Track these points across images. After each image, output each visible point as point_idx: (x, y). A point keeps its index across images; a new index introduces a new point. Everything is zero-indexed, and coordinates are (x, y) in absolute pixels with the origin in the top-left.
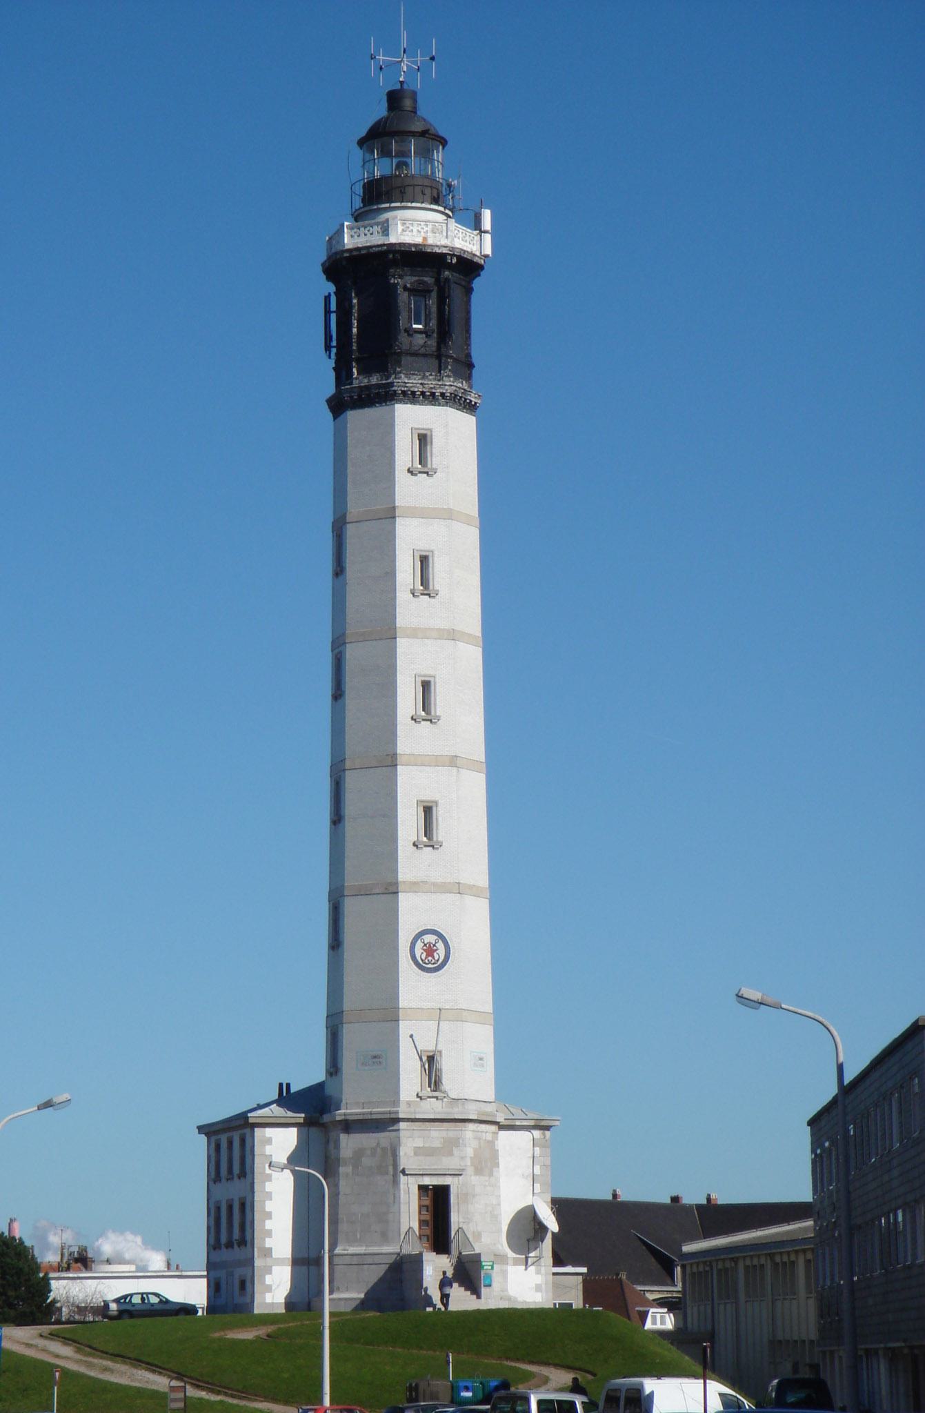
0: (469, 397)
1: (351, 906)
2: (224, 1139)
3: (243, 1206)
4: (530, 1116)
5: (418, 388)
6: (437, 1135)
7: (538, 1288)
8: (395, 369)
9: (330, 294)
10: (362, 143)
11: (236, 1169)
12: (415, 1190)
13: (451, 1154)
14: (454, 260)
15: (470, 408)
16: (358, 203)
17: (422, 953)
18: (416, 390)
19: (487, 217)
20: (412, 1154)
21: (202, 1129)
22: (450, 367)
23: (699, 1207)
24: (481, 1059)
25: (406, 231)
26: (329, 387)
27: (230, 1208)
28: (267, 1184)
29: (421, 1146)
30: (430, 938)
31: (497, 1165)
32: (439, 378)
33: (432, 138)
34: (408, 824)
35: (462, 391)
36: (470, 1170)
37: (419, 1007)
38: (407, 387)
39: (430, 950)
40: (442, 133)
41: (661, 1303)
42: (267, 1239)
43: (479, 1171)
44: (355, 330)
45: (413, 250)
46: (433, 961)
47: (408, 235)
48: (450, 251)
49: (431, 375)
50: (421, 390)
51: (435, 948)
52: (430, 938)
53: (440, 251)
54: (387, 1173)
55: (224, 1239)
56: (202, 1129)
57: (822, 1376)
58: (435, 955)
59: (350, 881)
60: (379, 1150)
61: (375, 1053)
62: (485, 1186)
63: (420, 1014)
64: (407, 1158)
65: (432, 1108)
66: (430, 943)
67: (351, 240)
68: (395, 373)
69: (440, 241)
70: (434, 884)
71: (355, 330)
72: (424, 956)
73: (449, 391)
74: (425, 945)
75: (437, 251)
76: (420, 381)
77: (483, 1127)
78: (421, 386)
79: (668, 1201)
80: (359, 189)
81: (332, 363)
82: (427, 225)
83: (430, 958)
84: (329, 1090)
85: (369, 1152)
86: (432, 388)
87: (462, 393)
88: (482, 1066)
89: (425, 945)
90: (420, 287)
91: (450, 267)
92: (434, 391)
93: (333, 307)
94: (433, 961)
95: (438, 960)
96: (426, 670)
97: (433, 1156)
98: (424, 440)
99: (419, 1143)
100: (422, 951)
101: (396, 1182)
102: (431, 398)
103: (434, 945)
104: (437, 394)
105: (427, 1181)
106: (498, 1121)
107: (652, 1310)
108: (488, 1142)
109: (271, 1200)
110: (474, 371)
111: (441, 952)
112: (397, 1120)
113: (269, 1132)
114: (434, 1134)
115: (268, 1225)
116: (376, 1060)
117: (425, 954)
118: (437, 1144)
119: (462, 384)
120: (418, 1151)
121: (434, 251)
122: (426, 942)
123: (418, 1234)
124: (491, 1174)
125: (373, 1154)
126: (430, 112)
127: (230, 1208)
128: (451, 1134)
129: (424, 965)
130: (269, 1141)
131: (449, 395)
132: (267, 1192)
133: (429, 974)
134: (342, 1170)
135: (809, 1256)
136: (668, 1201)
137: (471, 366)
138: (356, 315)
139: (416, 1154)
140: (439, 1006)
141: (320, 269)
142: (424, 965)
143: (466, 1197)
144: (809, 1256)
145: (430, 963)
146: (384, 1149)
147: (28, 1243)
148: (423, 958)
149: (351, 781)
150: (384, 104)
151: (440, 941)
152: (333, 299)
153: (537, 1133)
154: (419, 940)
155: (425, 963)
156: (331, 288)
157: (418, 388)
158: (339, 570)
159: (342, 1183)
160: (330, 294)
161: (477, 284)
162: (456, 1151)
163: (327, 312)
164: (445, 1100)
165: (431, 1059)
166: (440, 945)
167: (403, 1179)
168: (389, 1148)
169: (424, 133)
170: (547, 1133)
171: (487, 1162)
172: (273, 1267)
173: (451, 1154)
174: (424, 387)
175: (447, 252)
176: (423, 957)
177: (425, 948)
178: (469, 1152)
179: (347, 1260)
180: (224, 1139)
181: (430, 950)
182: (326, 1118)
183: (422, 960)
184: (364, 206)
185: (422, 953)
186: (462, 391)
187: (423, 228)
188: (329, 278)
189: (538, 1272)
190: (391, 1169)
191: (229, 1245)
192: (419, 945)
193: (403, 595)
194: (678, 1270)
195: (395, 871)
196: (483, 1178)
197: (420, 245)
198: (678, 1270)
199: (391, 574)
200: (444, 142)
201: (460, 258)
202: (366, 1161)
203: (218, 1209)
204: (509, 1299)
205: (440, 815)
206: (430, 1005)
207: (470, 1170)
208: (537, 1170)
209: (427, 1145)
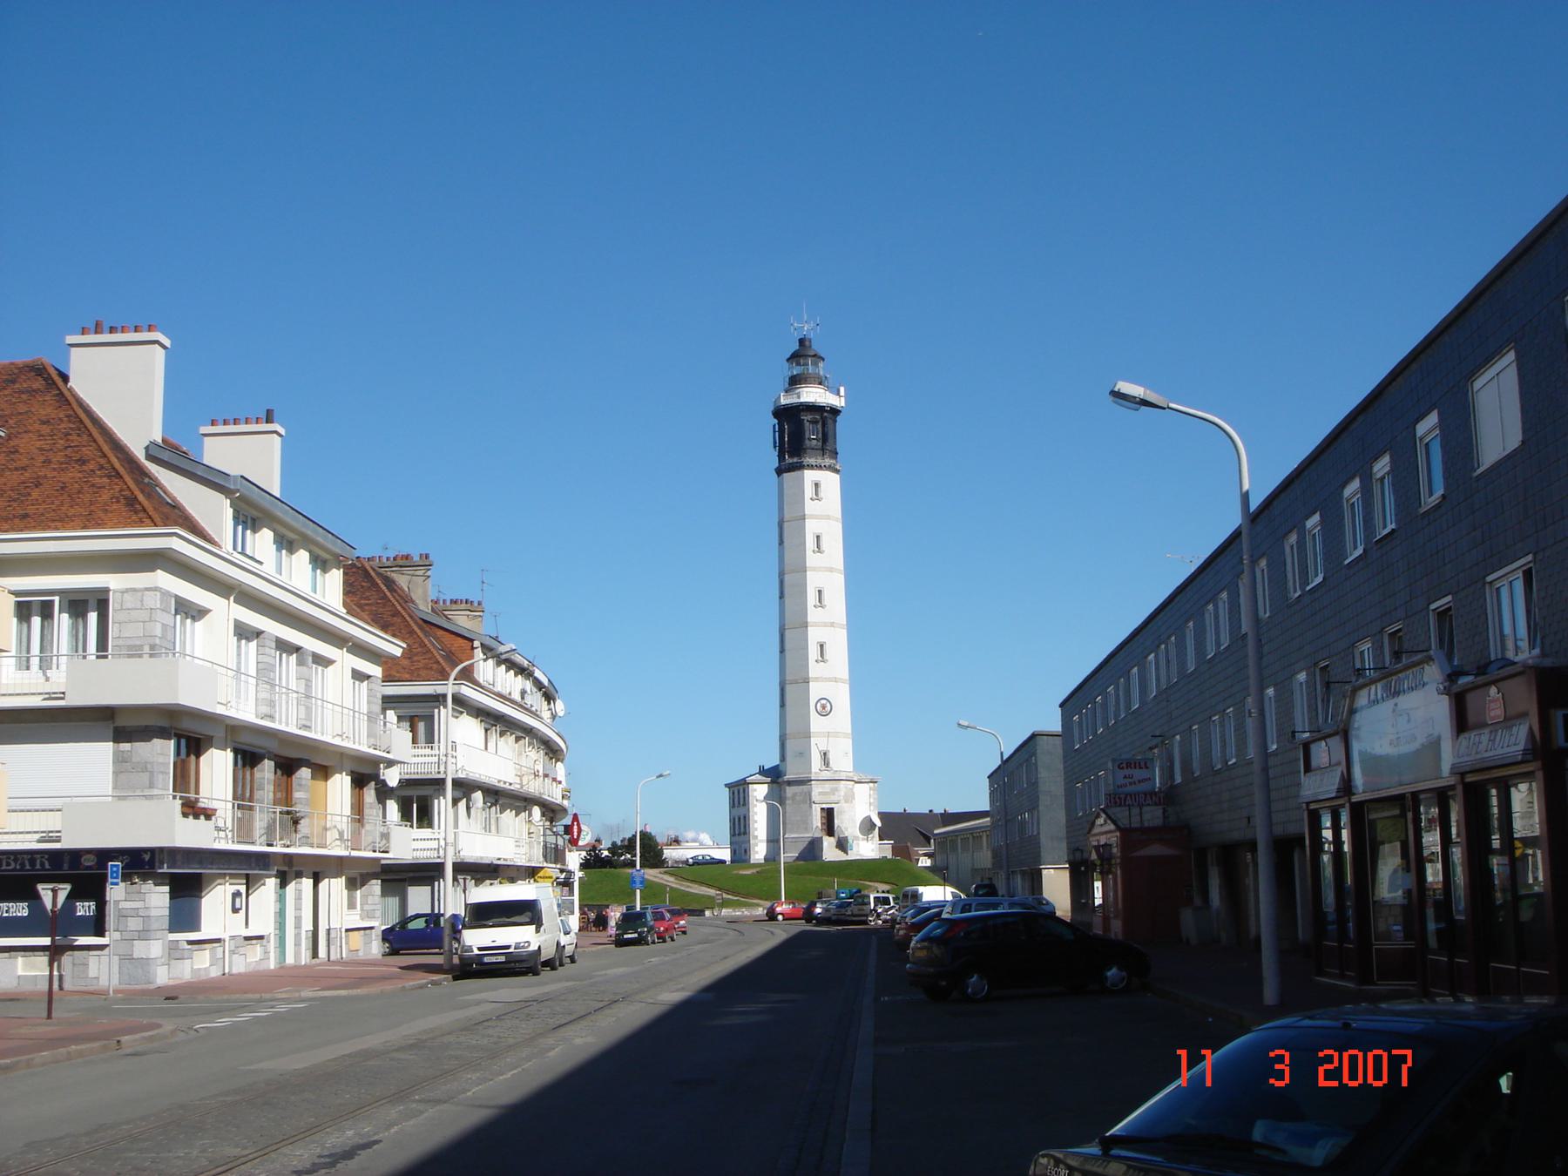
1: (788, 688)
2: (736, 789)
3: (745, 817)
4: (869, 777)
6: (828, 786)
10: (788, 360)
11: (741, 803)
12: (819, 810)
13: (834, 794)
15: (837, 471)
16: (787, 385)
19: (842, 390)
21: (726, 785)
23: (941, 814)
26: (774, 462)
27: (739, 819)
30: (824, 702)
31: (854, 799)
33: (818, 357)
34: (813, 652)
36: (843, 801)
39: (824, 707)
41: (925, 855)
43: (846, 802)
44: (786, 439)
52: (824, 702)
55: (737, 832)
56: (726, 785)
57: (994, 882)
59: (789, 677)
63: (820, 734)
64: (815, 796)
65: (826, 775)
67: (784, 401)
71: (786, 439)
79: (928, 812)
80: (787, 379)
84: (781, 768)
91: (827, 411)
93: (777, 429)
96: (820, 585)
98: (817, 485)
101: (811, 807)
102: (820, 467)
105: (824, 806)
107: (921, 858)
110: (838, 456)
112: (812, 780)
113: (755, 786)
114: (827, 786)
115: (756, 825)
120: (820, 793)
124: (852, 802)
126: (816, 347)
127: (739, 819)
128: (835, 786)
130: (755, 790)
134: (787, 802)
135: (988, 833)
136: (928, 812)
137: (837, 453)
141: (771, 414)
143: (841, 813)
144: (988, 833)
147: (653, 834)
149: (788, 634)
150: (798, 344)
152: (777, 426)
153: (871, 785)
156: (776, 421)
158: (781, 542)
159: (787, 807)
161: (839, 418)
162: (836, 793)
163: (774, 432)
165: (825, 754)
166: (828, 705)
167: (814, 805)
169: (815, 356)
170: (876, 785)
171: (850, 798)
173: (834, 794)
178: (842, 793)
179: (790, 840)
180: (736, 789)
181: (824, 707)
182: (780, 780)
188: (775, 417)
191: (739, 834)
192: (819, 705)
193: (809, 553)
194: (932, 841)
195: (808, 672)
198: (932, 841)
199: (804, 543)
200: (823, 360)
202: (798, 798)
203: (734, 819)
204: (860, 855)
205: (826, 648)
207: (843, 801)
208: (872, 801)
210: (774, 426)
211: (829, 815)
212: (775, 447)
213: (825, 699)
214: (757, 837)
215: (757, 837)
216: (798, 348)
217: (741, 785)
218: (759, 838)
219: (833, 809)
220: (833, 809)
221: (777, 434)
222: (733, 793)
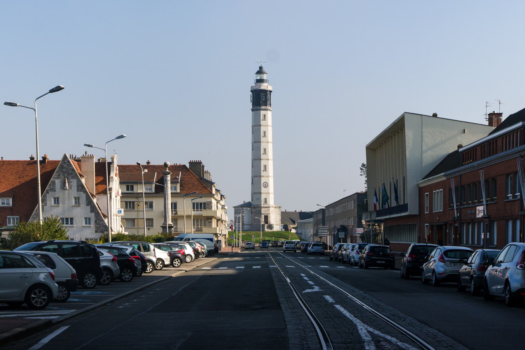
6: (266, 209)
7: (279, 228)
39: (265, 185)
40: (267, 73)
63: (264, 193)
64: (262, 212)
65: (266, 206)
81: (252, 104)
93: (252, 96)
96: (265, 147)
98: (265, 116)
99: (264, 210)
101: (261, 215)
105: (265, 215)
111: (267, 185)
120: (264, 211)
126: (265, 69)
150: (259, 68)
152: (252, 95)
156: (251, 93)
161: (271, 93)
163: (251, 97)
165: (266, 199)
166: (267, 184)
181: (265, 185)
192: (264, 184)
195: (261, 174)
202: (257, 212)
210: (251, 95)
211: (266, 217)
212: (251, 102)
213: (266, 182)
216: (259, 70)
217: (237, 207)
218: (245, 224)
219: (268, 216)
220: (268, 216)
221: (252, 97)
222: (236, 209)
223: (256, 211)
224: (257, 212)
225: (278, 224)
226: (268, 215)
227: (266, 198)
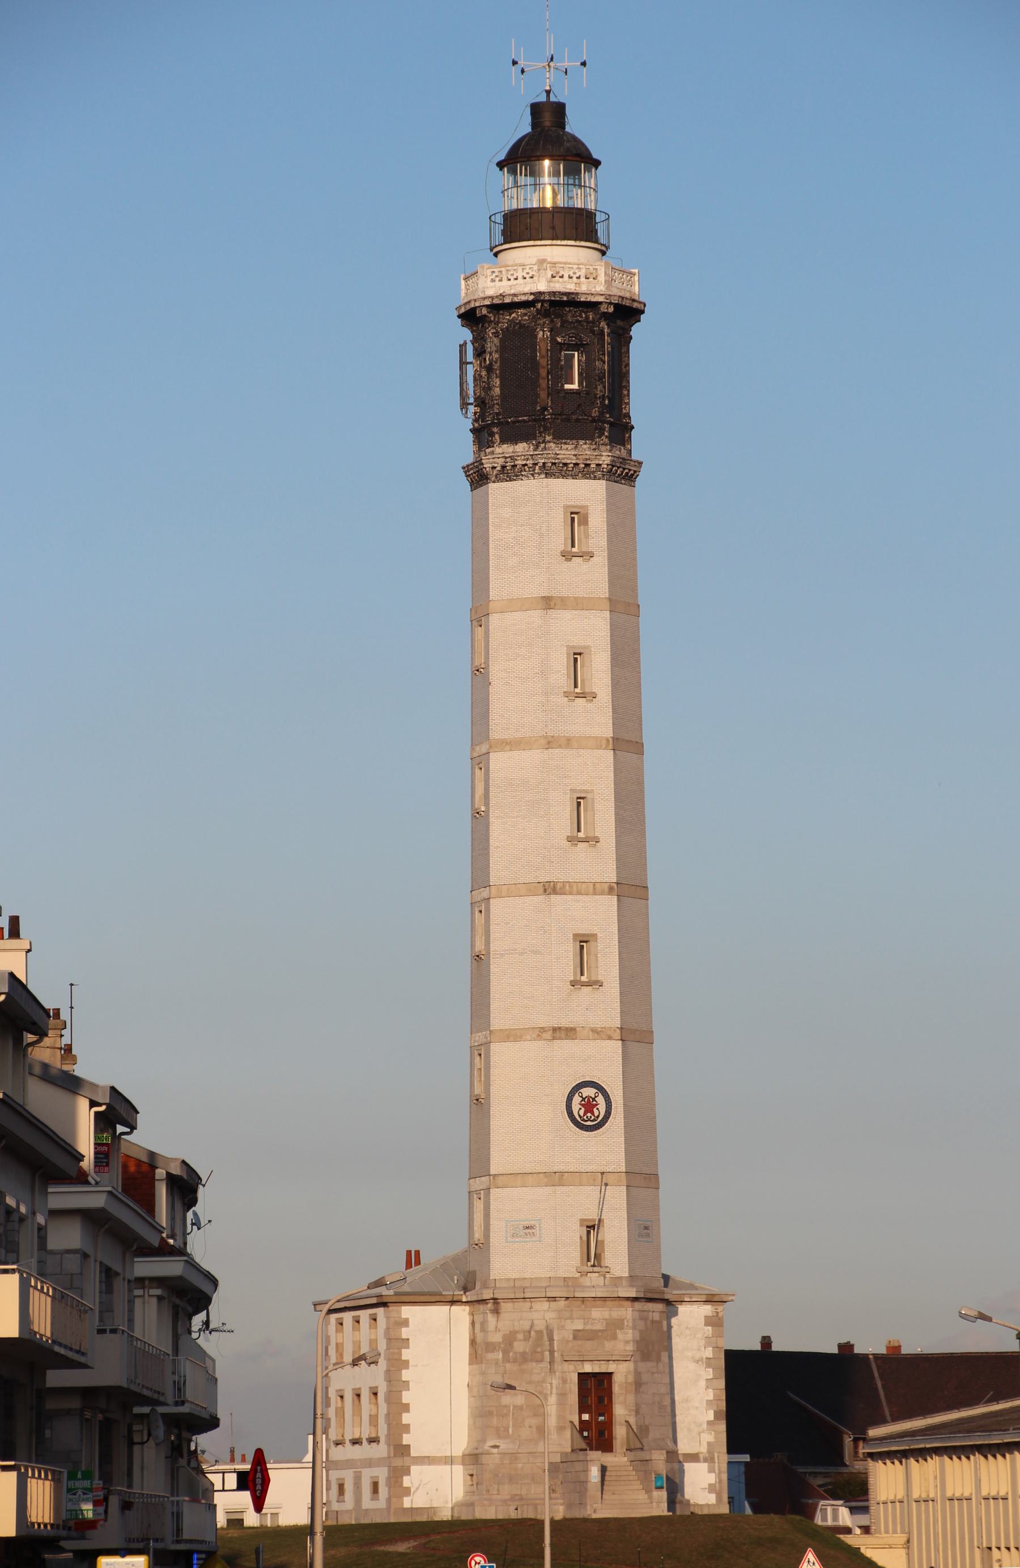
0: (627, 467)
5: (571, 459)
7: (711, 1488)
8: (545, 437)
9: (465, 343)
13: (614, 1337)
14: (611, 309)
17: (580, 1109)
18: (569, 461)
20: (571, 1336)
22: (606, 434)
24: (646, 1228)
25: (555, 277)
28: (404, 1372)
29: (582, 1329)
30: (589, 1092)
32: (594, 447)
35: (621, 460)
37: (577, 1170)
38: (558, 459)
39: (589, 1105)
42: (404, 1435)
45: (565, 298)
46: (593, 1117)
47: (558, 282)
48: (607, 299)
49: (586, 444)
50: (574, 462)
51: (594, 1102)
52: (589, 1092)
53: (595, 300)
54: (542, 1361)
58: (595, 1110)
60: (533, 1333)
61: (527, 1223)
62: (653, 1373)
66: (588, 1097)
68: (544, 442)
69: (595, 287)
70: (594, 1031)
72: (582, 1113)
73: (606, 462)
74: (584, 1099)
75: (592, 300)
76: (573, 453)
77: (650, 1306)
78: (574, 458)
82: (580, 268)
83: (589, 1115)
85: (520, 1336)
86: (587, 460)
87: (621, 463)
88: (648, 1235)
89: (584, 1099)
90: (572, 341)
92: (588, 462)
94: (593, 1117)
95: (599, 1116)
97: (594, 1340)
100: (580, 1107)
103: (594, 1099)
104: (592, 466)
106: (666, 1298)
108: (656, 1322)
109: (409, 1390)
116: (530, 1231)
117: (583, 1109)
118: (598, 1327)
119: (620, 451)
120: (577, 1335)
121: (588, 300)
122: (584, 1097)
123: (578, 1429)
125: (527, 1338)
129: (582, 1122)
131: (605, 466)
132: (404, 1381)
133: (588, 1133)
138: (498, 372)
139: (575, 1338)
140: (601, 1169)
142: (582, 1122)
145: (589, 1120)
146: (539, 1333)
148: (582, 1115)
151: (600, 1094)
154: (577, 1095)
155: (584, 1120)
156: (467, 335)
157: (571, 459)
160: (465, 343)
161: (636, 330)
164: (608, 1275)
166: (601, 1100)
168: (545, 1332)
172: (412, 1467)
173: (614, 1337)
174: (578, 459)
175: (603, 300)
176: (582, 1115)
177: (583, 1102)
181: (589, 1105)
183: (579, 1116)
184: (505, 243)
185: (580, 1109)
186: (621, 460)
187: (574, 273)
189: (711, 1470)
190: (547, 1353)
192: (576, 1100)
196: (649, 1364)
197: (572, 293)
201: (617, 306)
202: (519, 1346)
206: (590, 1168)
209: (588, 1327)
212: (464, 405)
214: (408, 1446)
215: (408, 1446)
218: (413, 1453)
219: (609, 1375)
220: (609, 1375)
223: (510, 1339)
224: (519, 1346)
225: (704, 1449)
226: (611, 1368)
227: (593, 1215)
